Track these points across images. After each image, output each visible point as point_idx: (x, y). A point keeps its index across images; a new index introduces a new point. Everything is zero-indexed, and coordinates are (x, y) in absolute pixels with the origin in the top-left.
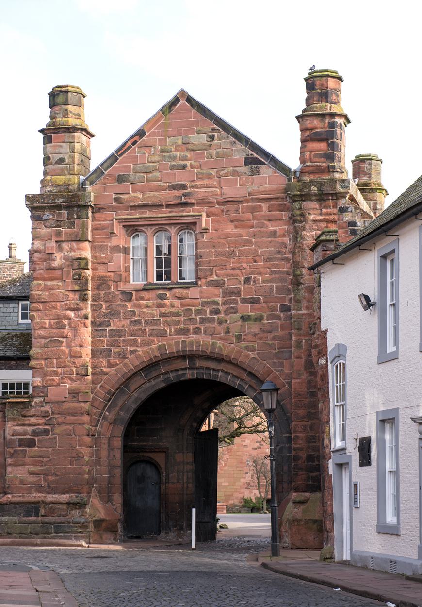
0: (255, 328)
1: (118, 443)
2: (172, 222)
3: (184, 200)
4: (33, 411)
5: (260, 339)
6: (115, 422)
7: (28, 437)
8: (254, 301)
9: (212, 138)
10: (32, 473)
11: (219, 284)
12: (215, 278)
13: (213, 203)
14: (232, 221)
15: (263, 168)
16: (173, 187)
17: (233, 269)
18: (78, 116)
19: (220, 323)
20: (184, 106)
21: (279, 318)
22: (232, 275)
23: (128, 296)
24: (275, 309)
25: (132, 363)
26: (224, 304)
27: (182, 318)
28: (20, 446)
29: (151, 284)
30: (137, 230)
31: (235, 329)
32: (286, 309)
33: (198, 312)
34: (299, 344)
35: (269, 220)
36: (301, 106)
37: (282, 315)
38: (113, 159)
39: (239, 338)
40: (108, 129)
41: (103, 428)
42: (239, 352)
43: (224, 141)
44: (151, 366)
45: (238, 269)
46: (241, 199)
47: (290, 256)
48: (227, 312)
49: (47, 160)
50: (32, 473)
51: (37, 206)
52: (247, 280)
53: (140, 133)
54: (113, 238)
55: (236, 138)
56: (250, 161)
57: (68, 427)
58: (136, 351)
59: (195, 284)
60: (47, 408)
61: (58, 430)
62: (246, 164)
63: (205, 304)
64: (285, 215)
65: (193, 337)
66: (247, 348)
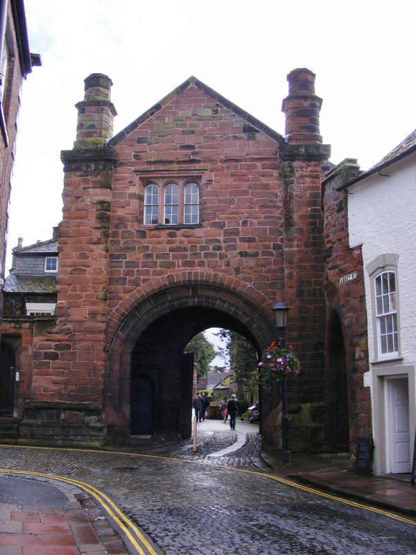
0: (251, 262)
1: (128, 359)
2: (181, 175)
3: (192, 157)
4: (56, 329)
5: (257, 272)
6: (124, 342)
7: (52, 350)
8: (250, 240)
9: (216, 112)
10: (55, 383)
11: (221, 225)
12: (217, 220)
13: (216, 161)
14: (232, 176)
15: (257, 135)
16: (183, 147)
17: (233, 213)
18: (107, 96)
19: (222, 257)
20: (192, 91)
21: (272, 254)
22: (232, 218)
23: (143, 234)
24: (268, 247)
25: (143, 290)
26: (225, 241)
27: (189, 253)
28: (45, 358)
29: (161, 225)
30: (150, 183)
31: (236, 261)
32: (277, 247)
33: (202, 248)
34: (290, 275)
35: (263, 176)
36: (286, 94)
37: (274, 252)
38: (134, 126)
39: (237, 270)
40: (128, 106)
41: (116, 346)
42: (238, 283)
43: (224, 113)
44: (159, 295)
45: (237, 213)
46: (240, 158)
47: (281, 204)
48: (227, 249)
49: (80, 126)
50: (55, 383)
51: (70, 160)
52: (245, 223)
53: (157, 107)
54: (131, 187)
55: (234, 111)
56: (247, 129)
57: (86, 343)
58: (147, 280)
59: (200, 226)
60: (70, 326)
61: (79, 346)
62: (244, 132)
63: (208, 241)
64: (275, 173)
65: (199, 269)
66: (244, 279)
